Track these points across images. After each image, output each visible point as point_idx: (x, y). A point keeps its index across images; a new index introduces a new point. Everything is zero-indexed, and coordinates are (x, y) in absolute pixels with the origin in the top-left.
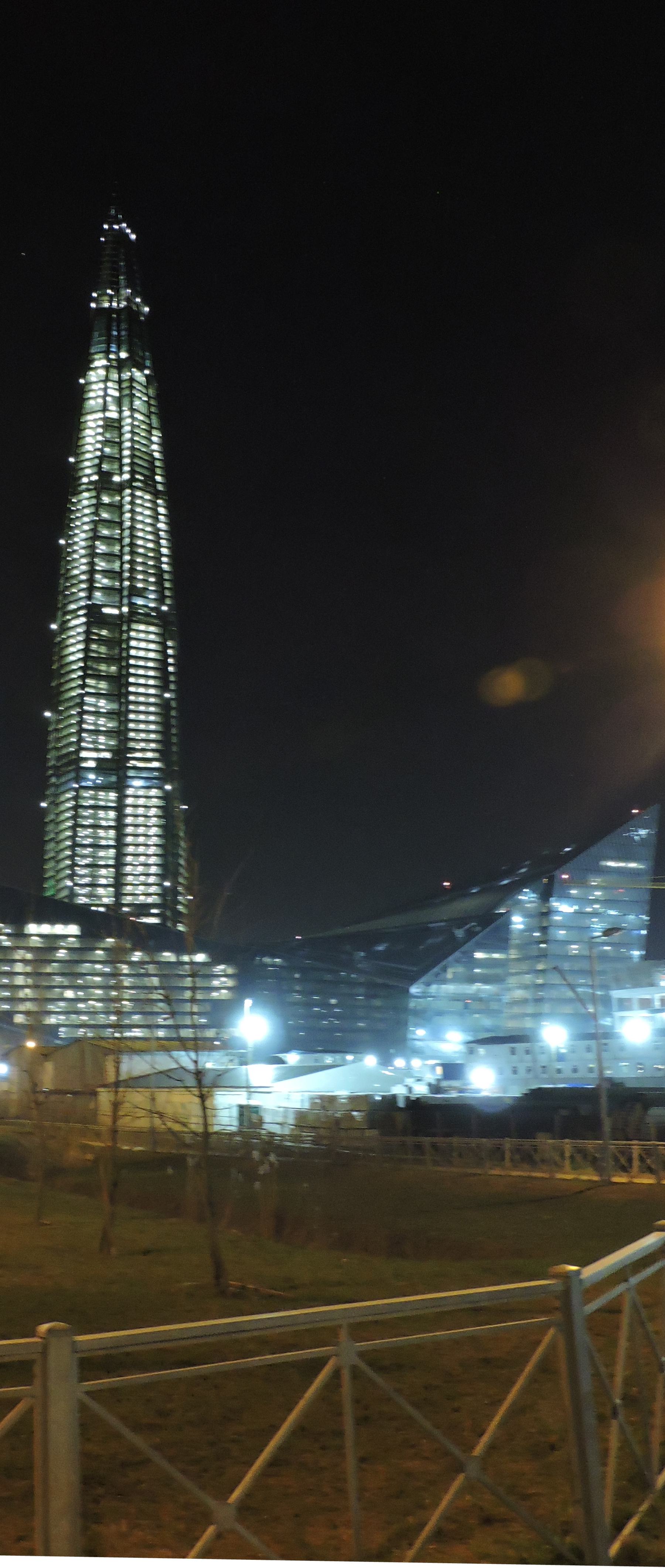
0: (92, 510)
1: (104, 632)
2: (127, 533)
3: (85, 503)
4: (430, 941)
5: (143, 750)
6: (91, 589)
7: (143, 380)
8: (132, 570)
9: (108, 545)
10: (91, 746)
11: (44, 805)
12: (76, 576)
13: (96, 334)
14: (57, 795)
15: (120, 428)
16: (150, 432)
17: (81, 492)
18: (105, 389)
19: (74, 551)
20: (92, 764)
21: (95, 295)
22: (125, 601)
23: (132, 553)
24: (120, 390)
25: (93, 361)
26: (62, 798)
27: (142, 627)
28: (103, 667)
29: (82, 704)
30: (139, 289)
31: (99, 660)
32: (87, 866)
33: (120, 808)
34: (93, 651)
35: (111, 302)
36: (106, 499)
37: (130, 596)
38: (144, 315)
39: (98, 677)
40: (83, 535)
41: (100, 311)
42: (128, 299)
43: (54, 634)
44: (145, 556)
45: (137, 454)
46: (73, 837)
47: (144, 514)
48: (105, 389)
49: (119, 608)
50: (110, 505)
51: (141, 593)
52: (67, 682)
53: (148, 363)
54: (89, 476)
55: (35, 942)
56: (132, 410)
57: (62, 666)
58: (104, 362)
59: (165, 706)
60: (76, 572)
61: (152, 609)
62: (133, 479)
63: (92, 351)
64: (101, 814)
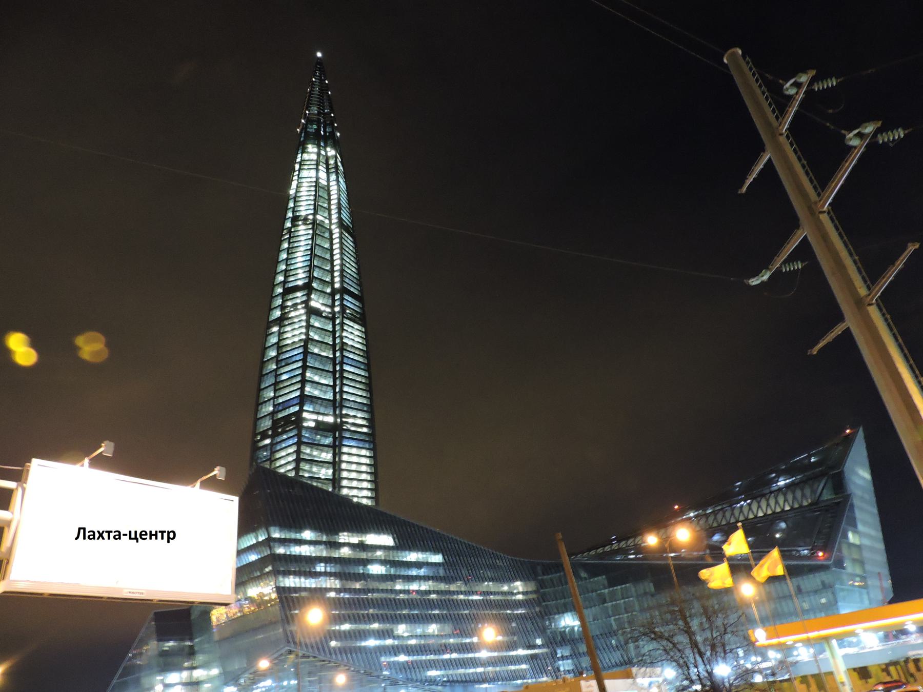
5: (355, 417)
14: (273, 452)
20: (312, 424)
22: (337, 303)
26: (278, 455)
33: (335, 464)
49: (332, 306)
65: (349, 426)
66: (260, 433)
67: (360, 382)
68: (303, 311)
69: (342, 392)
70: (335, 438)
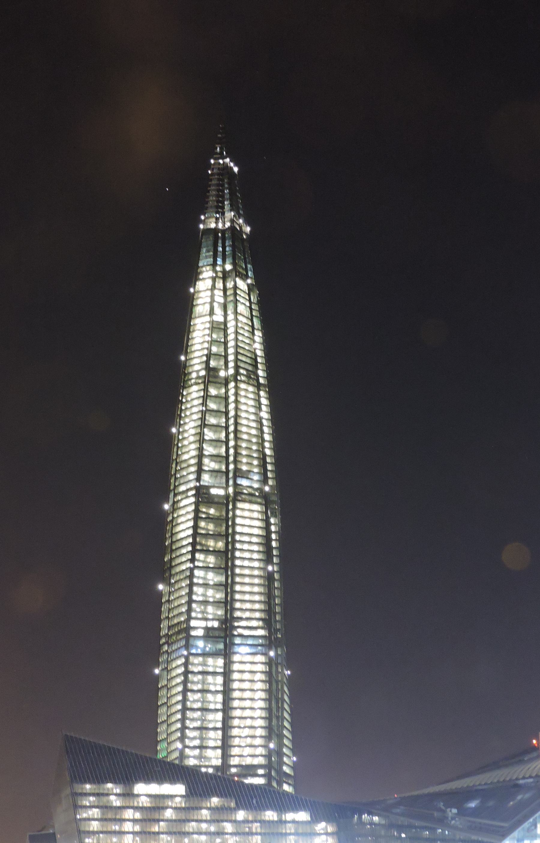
0: (201, 401)
1: (212, 511)
2: (232, 421)
3: (194, 395)
4: (519, 797)
5: (248, 619)
6: (200, 471)
7: (245, 288)
8: (236, 454)
9: (215, 432)
10: (200, 616)
12: (185, 461)
13: (204, 250)
14: (168, 662)
15: (225, 330)
16: (253, 334)
17: (192, 385)
18: (212, 296)
19: (184, 438)
21: (203, 217)
22: (231, 482)
23: (236, 438)
24: (225, 295)
25: (201, 272)
27: (246, 506)
28: (211, 543)
29: (191, 576)
30: (241, 212)
31: (207, 536)
32: (195, 729)
33: (227, 674)
34: (203, 529)
35: (217, 223)
36: (213, 391)
37: (235, 478)
38: (246, 234)
39: (206, 551)
40: (192, 424)
41: (208, 231)
42: (232, 221)
43: (167, 514)
44: (249, 441)
45: (241, 351)
46: (184, 701)
47: (247, 403)
48: (212, 296)
50: (216, 397)
51: (245, 475)
52: (177, 557)
53: (250, 274)
54: (198, 371)
55: (144, 801)
56: (236, 313)
57: (172, 543)
58: (211, 274)
59: (269, 578)
60: (185, 457)
61: (257, 489)
62: (237, 373)
63: (201, 264)
64: (210, 679)
68: (193, 500)
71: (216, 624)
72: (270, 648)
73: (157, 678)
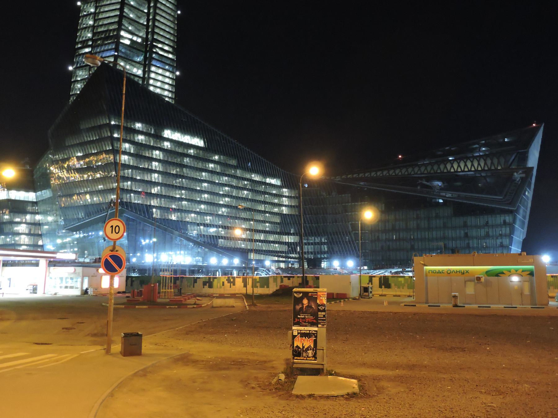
11: (71, 68)
20: (128, 42)
55: (167, 145)
65: (157, 49)
66: (81, 42)
67: (170, 14)
69: (154, 20)
70: (145, 58)
71: (139, 40)
72: (177, 71)
73: (71, 74)
